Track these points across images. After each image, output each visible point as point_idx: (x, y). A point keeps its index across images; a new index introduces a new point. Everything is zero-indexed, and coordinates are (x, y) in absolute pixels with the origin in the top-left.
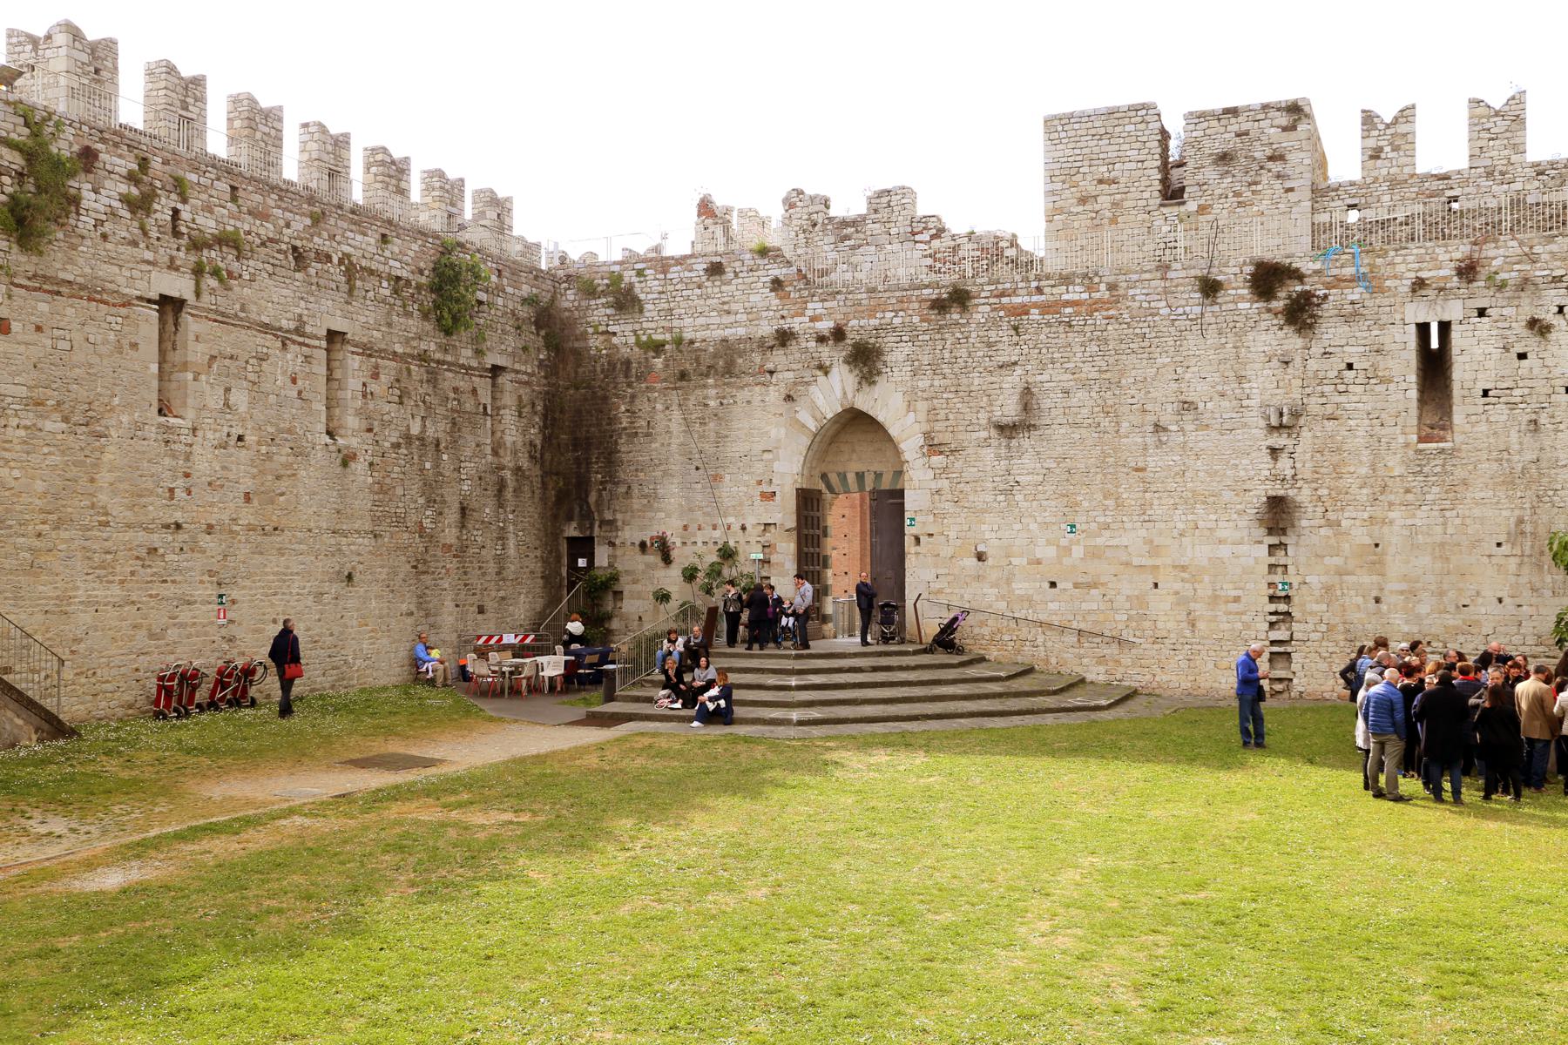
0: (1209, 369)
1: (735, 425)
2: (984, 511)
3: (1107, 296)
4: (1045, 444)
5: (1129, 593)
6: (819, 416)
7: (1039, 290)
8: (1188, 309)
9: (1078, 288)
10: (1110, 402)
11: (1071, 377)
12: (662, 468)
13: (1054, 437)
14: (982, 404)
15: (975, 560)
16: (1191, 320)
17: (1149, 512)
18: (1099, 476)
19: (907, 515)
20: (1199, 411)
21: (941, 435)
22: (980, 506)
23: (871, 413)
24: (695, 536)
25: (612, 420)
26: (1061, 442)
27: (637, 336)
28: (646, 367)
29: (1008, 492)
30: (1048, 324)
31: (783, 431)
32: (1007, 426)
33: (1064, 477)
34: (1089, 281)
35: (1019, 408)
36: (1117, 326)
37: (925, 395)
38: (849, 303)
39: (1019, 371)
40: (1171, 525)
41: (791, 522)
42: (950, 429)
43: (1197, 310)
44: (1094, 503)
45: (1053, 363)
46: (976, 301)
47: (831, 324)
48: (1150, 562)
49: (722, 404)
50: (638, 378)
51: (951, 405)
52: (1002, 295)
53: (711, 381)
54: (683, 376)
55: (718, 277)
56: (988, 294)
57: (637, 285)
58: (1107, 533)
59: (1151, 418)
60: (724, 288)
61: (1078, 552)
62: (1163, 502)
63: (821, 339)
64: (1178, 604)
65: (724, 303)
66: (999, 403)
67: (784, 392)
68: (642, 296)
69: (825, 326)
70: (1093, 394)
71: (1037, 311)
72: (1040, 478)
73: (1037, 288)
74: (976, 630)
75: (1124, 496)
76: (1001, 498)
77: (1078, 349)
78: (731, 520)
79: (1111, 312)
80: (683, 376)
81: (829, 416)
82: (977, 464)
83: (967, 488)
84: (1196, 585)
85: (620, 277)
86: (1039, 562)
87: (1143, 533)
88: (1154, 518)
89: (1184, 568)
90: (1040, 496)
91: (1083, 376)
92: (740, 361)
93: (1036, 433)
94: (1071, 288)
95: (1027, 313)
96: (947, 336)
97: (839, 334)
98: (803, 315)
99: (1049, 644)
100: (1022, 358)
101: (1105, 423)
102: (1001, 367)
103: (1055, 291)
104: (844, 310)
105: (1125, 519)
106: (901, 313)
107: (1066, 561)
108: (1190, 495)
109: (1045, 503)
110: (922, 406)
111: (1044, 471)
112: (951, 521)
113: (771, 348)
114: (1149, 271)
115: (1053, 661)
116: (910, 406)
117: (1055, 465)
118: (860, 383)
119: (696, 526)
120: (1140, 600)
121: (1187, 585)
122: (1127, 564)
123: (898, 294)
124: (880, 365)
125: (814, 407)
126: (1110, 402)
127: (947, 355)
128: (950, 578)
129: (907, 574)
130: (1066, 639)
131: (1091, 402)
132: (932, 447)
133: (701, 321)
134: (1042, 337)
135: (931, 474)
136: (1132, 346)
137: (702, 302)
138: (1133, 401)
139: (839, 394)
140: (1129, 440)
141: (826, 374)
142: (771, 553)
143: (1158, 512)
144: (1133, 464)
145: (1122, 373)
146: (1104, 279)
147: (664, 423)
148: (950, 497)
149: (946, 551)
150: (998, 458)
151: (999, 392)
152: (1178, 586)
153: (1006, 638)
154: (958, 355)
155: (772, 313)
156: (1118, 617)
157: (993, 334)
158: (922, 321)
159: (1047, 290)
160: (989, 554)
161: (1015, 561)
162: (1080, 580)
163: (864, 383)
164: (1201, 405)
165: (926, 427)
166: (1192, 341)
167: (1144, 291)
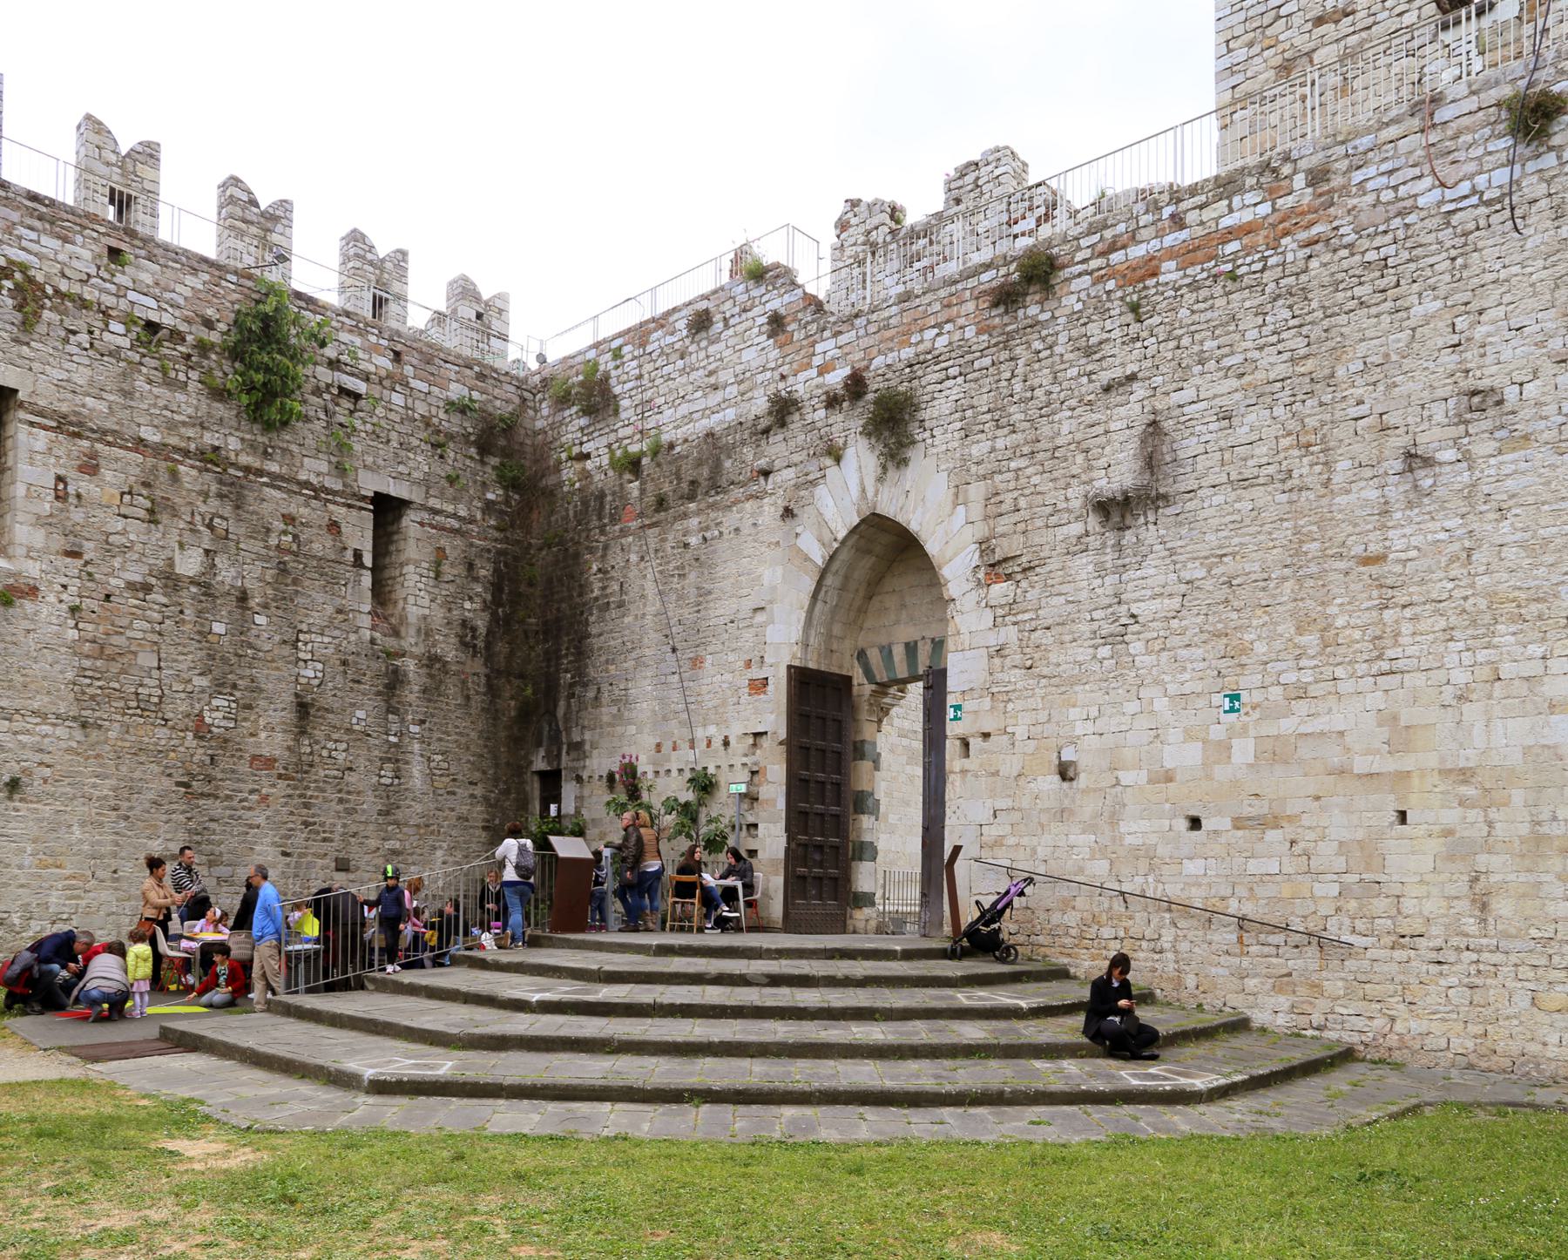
0: (1531, 303)
1: (720, 571)
2: (1074, 681)
3: (1306, 200)
4: (1184, 531)
5: (1346, 835)
6: (827, 537)
7: (1178, 222)
8: (1481, 181)
9: (1250, 198)
10: (1311, 422)
11: (1234, 383)
12: (634, 655)
13: (1202, 514)
14: (1075, 470)
15: (1057, 778)
16: (1488, 203)
17: (1390, 653)
18: (1289, 585)
19: (951, 700)
20: (1508, 407)
21: (1004, 542)
22: (1067, 670)
23: (899, 519)
24: (668, 760)
25: (583, 588)
26: (1214, 522)
27: (612, 452)
28: (621, 497)
29: (1118, 638)
30: (1194, 286)
31: (779, 570)
32: (1112, 500)
33: (1221, 594)
34: (1269, 174)
35: (1138, 465)
36: (1327, 258)
37: (982, 470)
38: (872, 329)
39: (1139, 390)
40: (1440, 676)
41: (783, 734)
42: (1021, 527)
43: (1501, 176)
44: (1278, 645)
45: (1201, 362)
46: (1066, 273)
47: (847, 371)
48: (1390, 765)
49: (705, 539)
50: (614, 520)
51: (1023, 481)
52: (1113, 247)
53: (692, 506)
54: (661, 503)
55: (704, 334)
56: (1086, 253)
57: (613, 373)
58: (1301, 707)
59: (1398, 441)
60: (712, 349)
61: (1243, 751)
62: (1423, 626)
63: (832, 402)
64: (1451, 858)
65: (711, 374)
66: (1103, 462)
67: (781, 503)
68: (617, 390)
69: (837, 378)
70: (1279, 411)
71: (1172, 265)
72: (1175, 603)
73: (1172, 216)
74: (1056, 918)
75: (1340, 622)
76: (1105, 651)
77: (1249, 322)
78: (712, 730)
79: (1315, 230)
80: (661, 503)
81: (841, 535)
82: (1064, 588)
83: (1045, 638)
84: (1493, 814)
85: (596, 364)
86: (1169, 778)
87: (1376, 700)
88: (1400, 664)
89: (1465, 775)
90: (1174, 641)
91: (1260, 376)
92: (728, 464)
93: (1169, 511)
94: (1236, 200)
95: (1154, 274)
96: (1018, 350)
97: (856, 385)
98: (809, 366)
99: (1184, 946)
100: (1148, 363)
101: (1303, 468)
102: (1107, 389)
103: (1207, 214)
104: (865, 342)
105: (1340, 672)
106: (948, 327)
107: (1221, 773)
108: (1483, 604)
109: (1183, 653)
110: (977, 491)
111: (1183, 588)
112: (1019, 705)
113: (766, 431)
114: (1395, 121)
115: (1190, 981)
116: (958, 496)
117: (1201, 573)
118: (884, 468)
119: (670, 744)
120: (1367, 852)
121: (1473, 815)
122: (1342, 772)
123: (942, 293)
124: (914, 428)
125: (822, 522)
126: (1311, 422)
127: (1018, 387)
128: (1017, 816)
129: (948, 812)
130: (1216, 937)
131: (1276, 430)
132: (995, 567)
133: (684, 409)
134: (1184, 312)
135: (988, 616)
136: (1358, 291)
137: (684, 379)
138: (1363, 410)
139: (855, 492)
140: (1352, 497)
141: (838, 460)
142: (758, 786)
143: (1410, 651)
144: (1358, 550)
145: (1338, 353)
146: (1303, 164)
147: (639, 582)
148: (1018, 659)
149: (1011, 766)
150: (1101, 572)
151: (1103, 439)
152: (1451, 816)
153: (1107, 932)
154: (1036, 382)
155: (769, 374)
156: (1320, 890)
157: (1093, 329)
158: (978, 333)
159: (1191, 218)
160: (1081, 765)
161: (1127, 777)
162: (1247, 811)
163: (890, 465)
164: (1511, 393)
165: (981, 530)
166: (1490, 250)
167: (1385, 167)
